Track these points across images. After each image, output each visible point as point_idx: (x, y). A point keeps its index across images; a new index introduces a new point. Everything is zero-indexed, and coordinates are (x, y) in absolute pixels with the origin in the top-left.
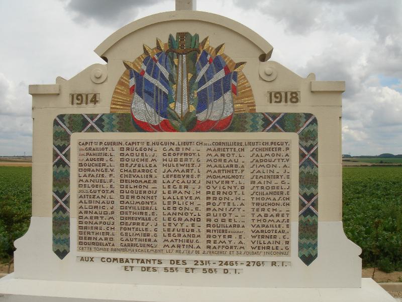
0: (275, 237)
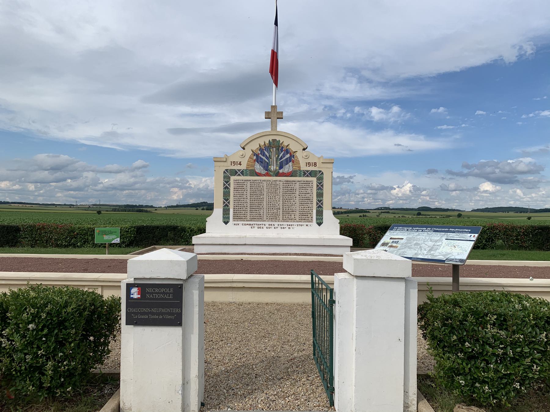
0: (307, 215)
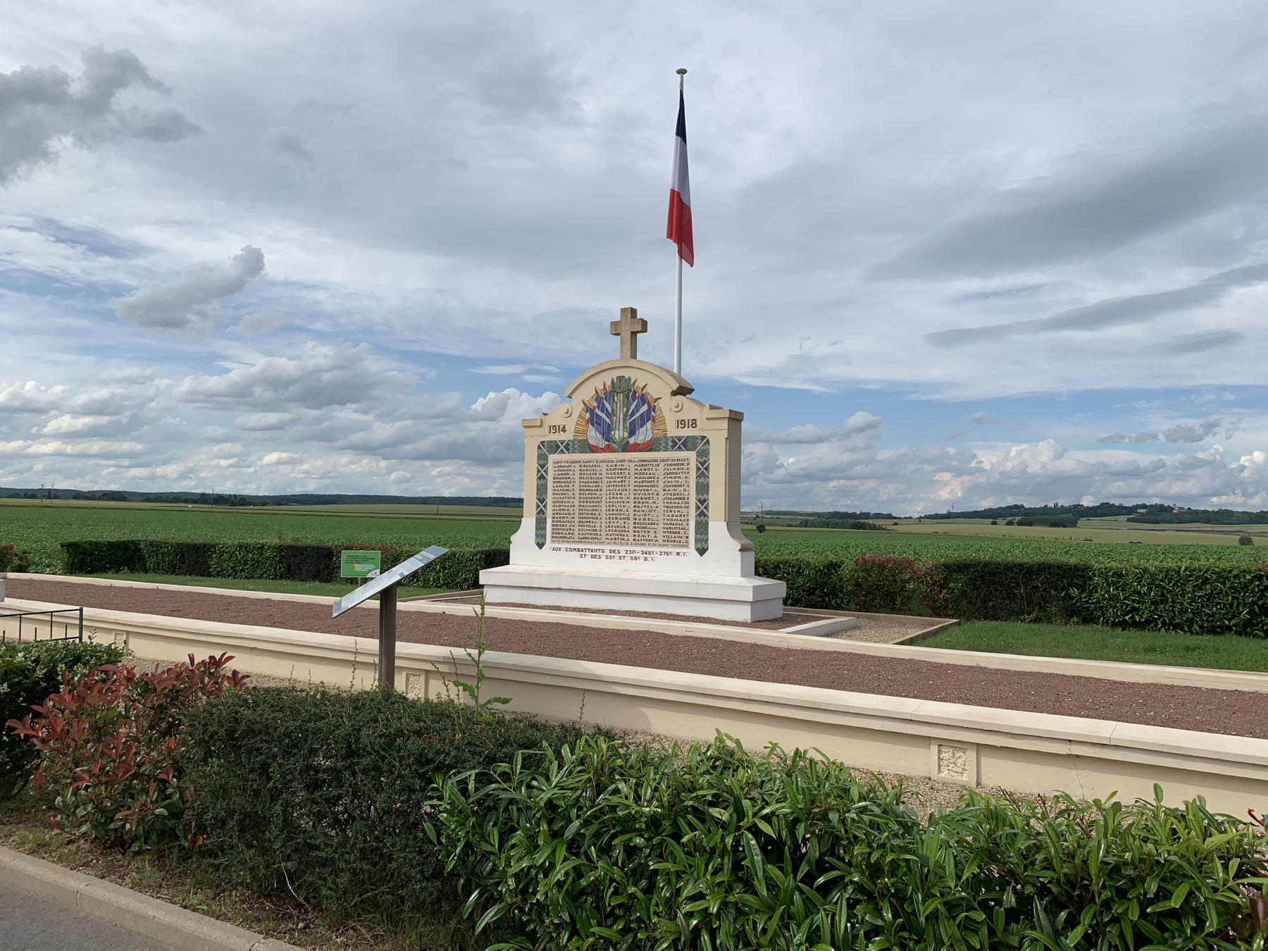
0: (679, 533)
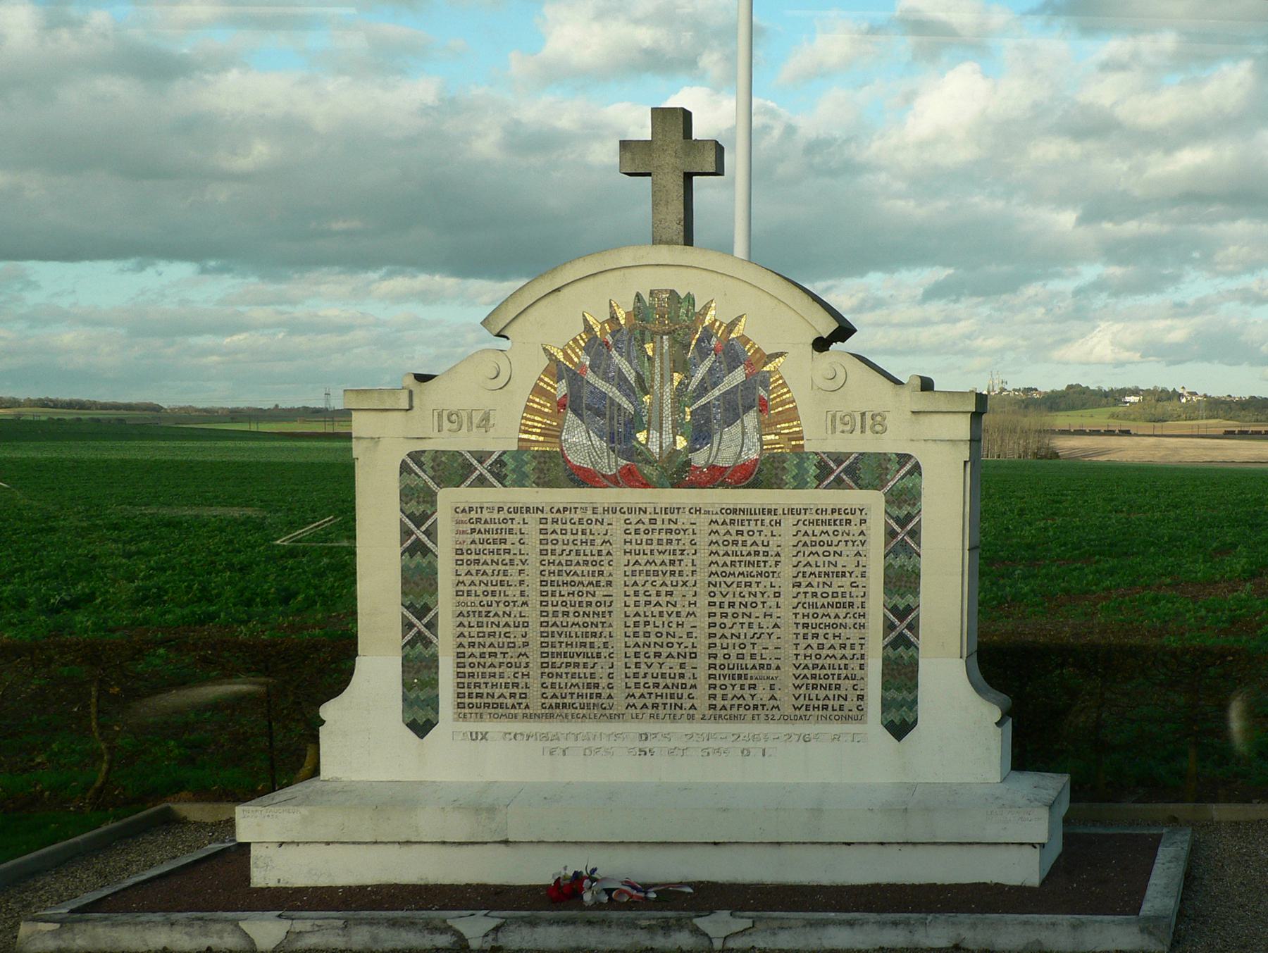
0: (838, 687)
